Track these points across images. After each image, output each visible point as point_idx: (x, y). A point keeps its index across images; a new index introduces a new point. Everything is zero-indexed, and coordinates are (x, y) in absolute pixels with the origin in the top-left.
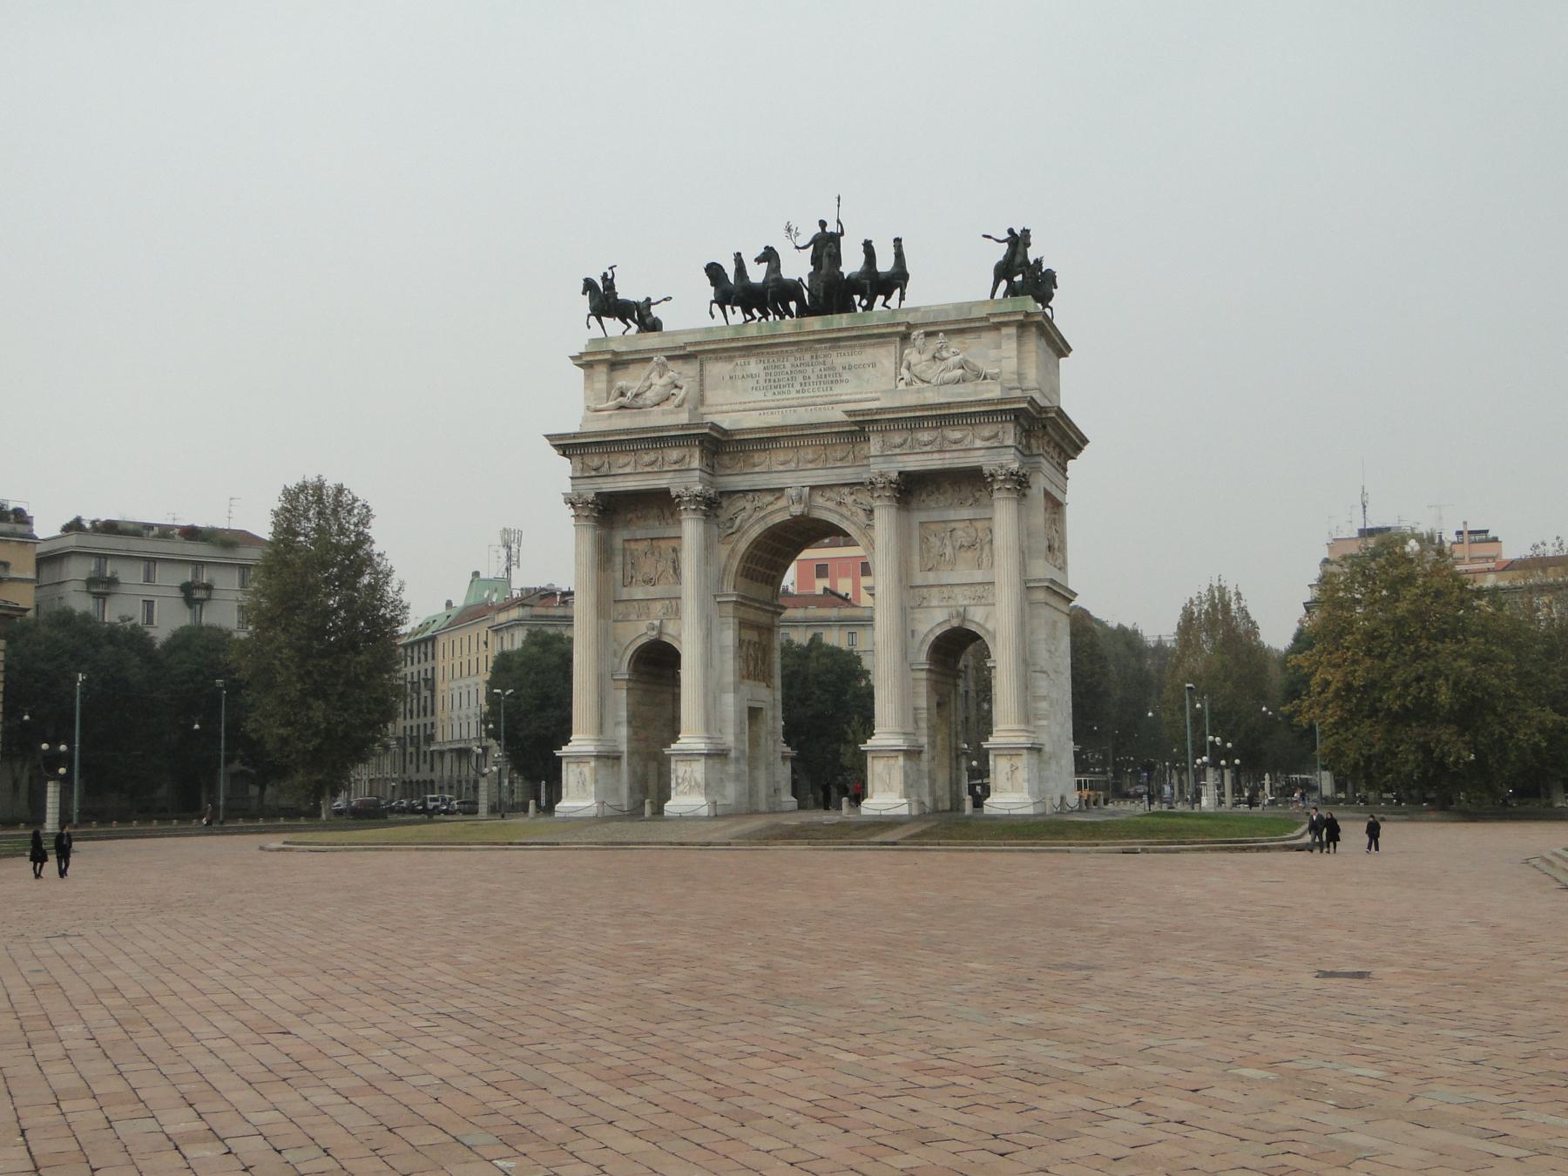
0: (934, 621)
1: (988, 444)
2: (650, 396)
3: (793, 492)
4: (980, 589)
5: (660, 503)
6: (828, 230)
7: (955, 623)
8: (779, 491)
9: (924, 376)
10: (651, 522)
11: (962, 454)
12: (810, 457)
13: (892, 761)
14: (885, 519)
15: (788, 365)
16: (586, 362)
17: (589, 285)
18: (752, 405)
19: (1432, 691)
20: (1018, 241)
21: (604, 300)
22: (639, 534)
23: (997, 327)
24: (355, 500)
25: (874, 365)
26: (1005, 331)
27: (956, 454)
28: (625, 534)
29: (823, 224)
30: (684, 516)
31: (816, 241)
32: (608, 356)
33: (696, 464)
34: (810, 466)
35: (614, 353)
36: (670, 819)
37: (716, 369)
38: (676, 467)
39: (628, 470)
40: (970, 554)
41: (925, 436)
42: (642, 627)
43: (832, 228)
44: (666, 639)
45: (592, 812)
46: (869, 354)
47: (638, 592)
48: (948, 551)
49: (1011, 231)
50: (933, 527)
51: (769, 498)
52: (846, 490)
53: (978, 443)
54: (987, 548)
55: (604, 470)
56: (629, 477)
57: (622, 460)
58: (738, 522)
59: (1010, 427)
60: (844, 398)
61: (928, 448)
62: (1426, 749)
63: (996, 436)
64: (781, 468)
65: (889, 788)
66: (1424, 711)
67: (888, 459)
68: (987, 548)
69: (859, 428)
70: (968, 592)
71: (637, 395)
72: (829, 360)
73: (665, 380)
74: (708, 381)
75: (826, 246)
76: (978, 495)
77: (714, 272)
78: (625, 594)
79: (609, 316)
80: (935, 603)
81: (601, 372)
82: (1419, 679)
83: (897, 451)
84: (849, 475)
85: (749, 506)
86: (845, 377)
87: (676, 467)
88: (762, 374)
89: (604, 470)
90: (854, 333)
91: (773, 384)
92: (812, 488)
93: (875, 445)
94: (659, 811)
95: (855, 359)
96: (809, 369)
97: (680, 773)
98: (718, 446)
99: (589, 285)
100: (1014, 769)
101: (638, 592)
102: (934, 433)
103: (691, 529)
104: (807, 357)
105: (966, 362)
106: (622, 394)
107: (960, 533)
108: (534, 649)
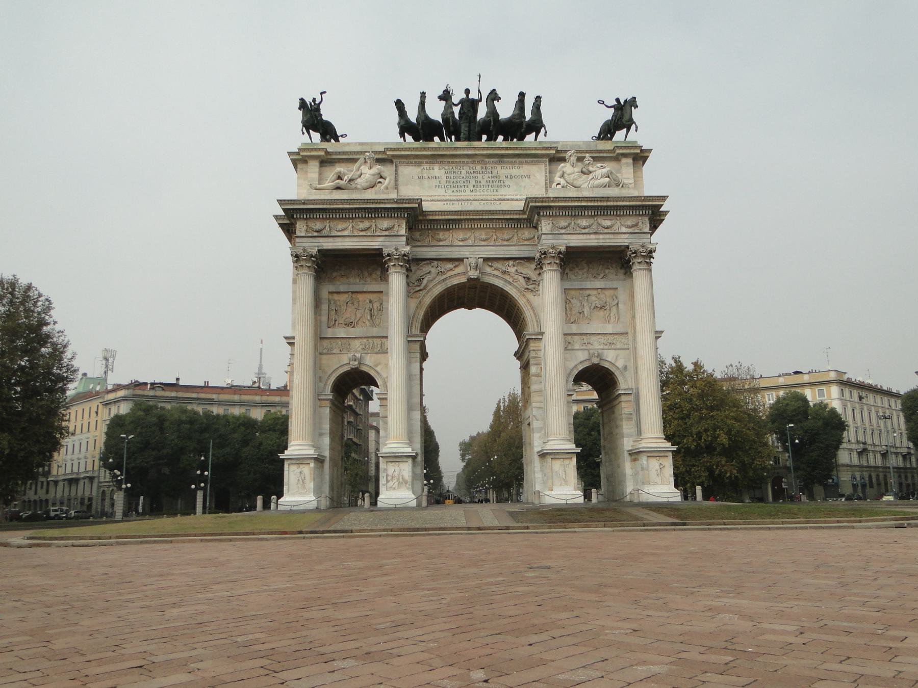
0: (580, 359)
1: (630, 230)
2: (361, 182)
3: (473, 261)
4: (611, 338)
5: (372, 262)
6: (471, 96)
7: (595, 361)
8: (460, 260)
9: (577, 183)
10: (351, 280)
11: (611, 236)
12: (483, 237)
13: (567, 462)
14: (550, 281)
15: (464, 172)
16: (299, 160)
17: (303, 104)
18: (436, 198)
19: (715, 438)
21: (313, 118)
24: (40, 295)
25: (529, 177)
26: (624, 160)
27: (607, 236)
28: (332, 288)
29: (467, 91)
30: (392, 270)
31: (462, 102)
32: (322, 153)
33: (403, 231)
34: (483, 243)
35: (327, 153)
36: (381, 510)
38: (387, 233)
39: (345, 233)
40: (601, 313)
41: (584, 222)
42: (345, 359)
43: (474, 95)
45: (313, 505)
46: (525, 169)
47: (341, 332)
48: (586, 310)
49: (618, 100)
50: (573, 292)
51: (449, 266)
52: (511, 263)
53: (624, 230)
54: (614, 309)
55: (325, 233)
56: (347, 238)
57: (341, 225)
58: (425, 281)
59: (646, 220)
60: (507, 197)
61: (586, 231)
62: (711, 471)
63: (637, 225)
64: (461, 243)
65: (566, 482)
66: (710, 449)
67: (555, 236)
68: (614, 309)
69: (534, 213)
70: (603, 339)
71: (351, 180)
72: (495, 172)
74: (401, 179)
76: (607, 271)
77: (399, 105)
78: (330, 333)
79: (314, 130)
80: (577, 346)
81: (314, 166)
82: (706, 430)
83: (563, 231)
84: (513, 251)
85: (433, 270)
86: (507, 183)
87: (387, 233)
88: (444, 177)
89: (325, 233)
90: (517, 152)
91: (451, 184)
93: (545, 226)
94: (374, 503)
95: (515, 171)
96: (480, 176)
97: (390, 472)
99: (303, 104)
100: (662, 467)
101: (341, 332)
102: (591, 221)
104: (479, 168)
105: (611, 173)
106: (340, 178)
107: (593, 298)
108: (140, 413)
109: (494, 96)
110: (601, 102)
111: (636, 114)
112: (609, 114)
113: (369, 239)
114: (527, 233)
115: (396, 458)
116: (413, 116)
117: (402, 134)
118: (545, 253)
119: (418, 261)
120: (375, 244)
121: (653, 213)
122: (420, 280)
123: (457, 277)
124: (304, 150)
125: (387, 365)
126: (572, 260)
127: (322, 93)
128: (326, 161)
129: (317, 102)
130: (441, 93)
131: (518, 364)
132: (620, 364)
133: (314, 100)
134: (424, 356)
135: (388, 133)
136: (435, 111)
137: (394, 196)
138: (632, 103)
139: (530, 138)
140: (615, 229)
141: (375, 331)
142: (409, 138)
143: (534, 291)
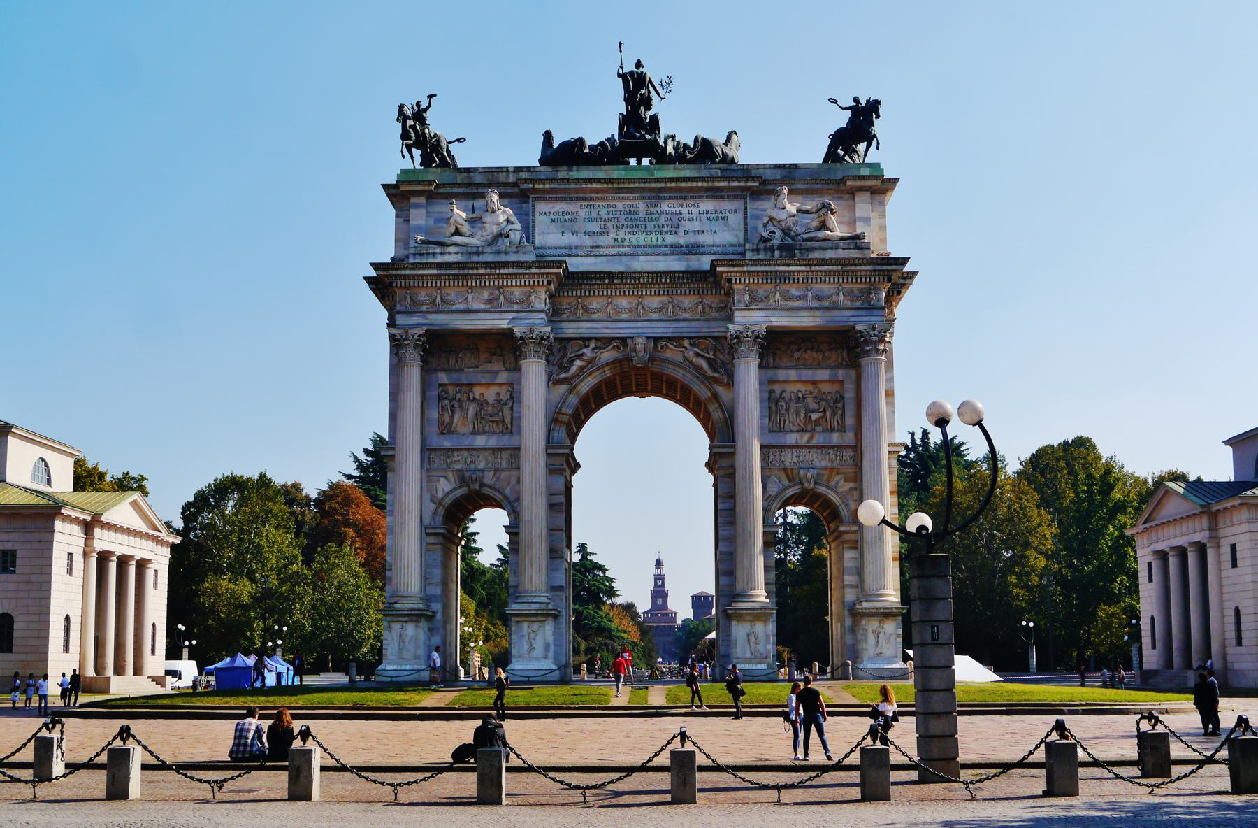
16: (398, 193)
34: (655, 316)
44: (486, 491)
49: (856, 100)
92: (656, 340)
110: (833, 101)
111: (878, 127)
113: (497, 315)
118: (737, 337)
119: (564, 342)
121: (893, 276)
124: (408, 183)
126: (775, 345)
127: (430, 97)
129: (423, 106)
131: (711, 478)
133: (418, 104)
134: (575, 467)
138: (873, 106)
141: (505, 441)
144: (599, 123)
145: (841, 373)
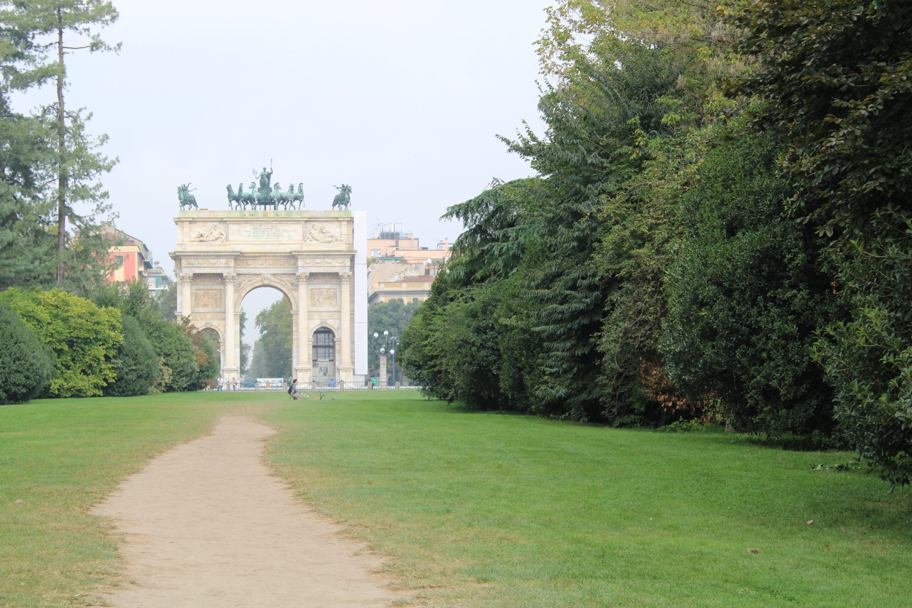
0: (316, 324)
2: (211, 238)
20: (346, 190)
22: (202, 287)
23: (340, 221)
29: (265, 169)
37: (233, 227)
41: (319, 261)
43: (268, 170)
47: (202, 310)
67: (305, 267)
70: (328, 314)
73: (218, 232)
75: (266, 178)
77: (229, 189)
84: (286, 271)
93: (300, 263)
98: (239, 257)
101: (202, 310)
103: (230, 289)
106: (202, 236)
109: (277, 186)
112: (338, 192)
114: (292, 261)
115: (230, 371)
116: (236, 192)
117: (230, 205)
120: (219, 271)
122: (240, 284)
123: (257, 281)
125: (225, 327)
128: (193, 221)
130: (250, 185)
132: (336, 326)
135: (221, 205)
136: (247, 191)
137: (227, 248)
139: (297, 202)
140: (332, 264)
141: (218, 309)
142: (234, 203)
143: (297, 290)
144: (249, 185)
145: (336, 286)
